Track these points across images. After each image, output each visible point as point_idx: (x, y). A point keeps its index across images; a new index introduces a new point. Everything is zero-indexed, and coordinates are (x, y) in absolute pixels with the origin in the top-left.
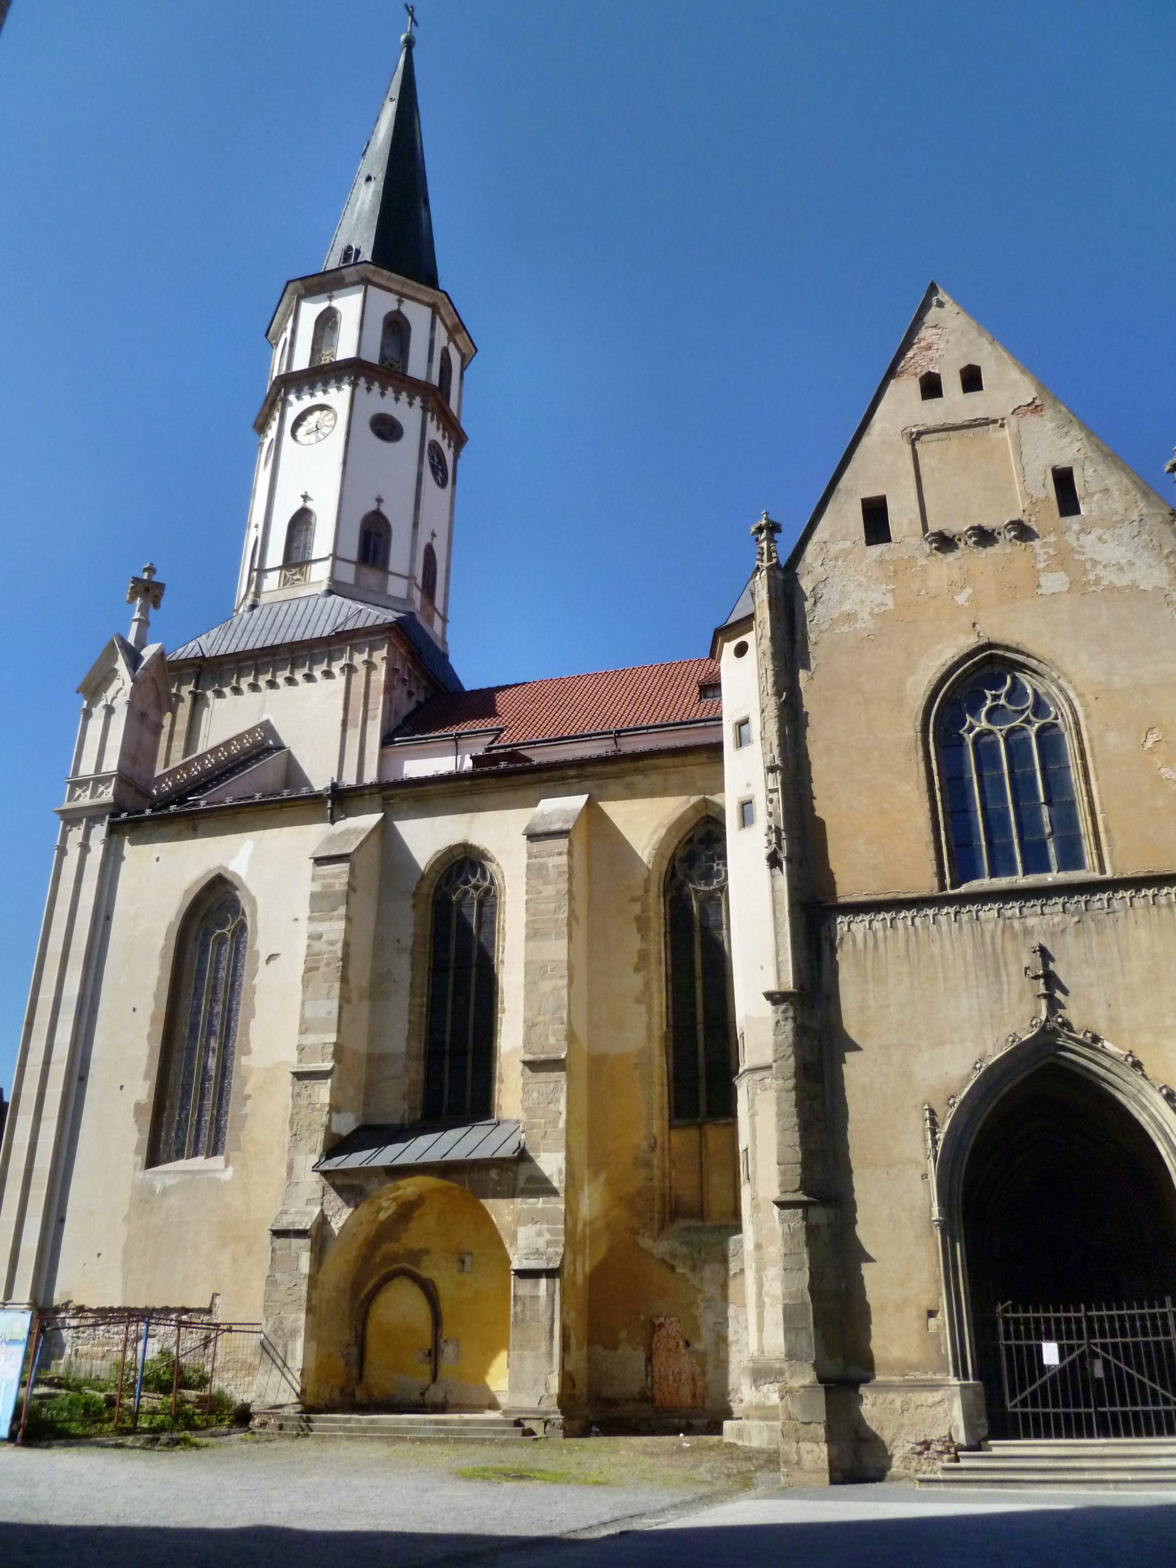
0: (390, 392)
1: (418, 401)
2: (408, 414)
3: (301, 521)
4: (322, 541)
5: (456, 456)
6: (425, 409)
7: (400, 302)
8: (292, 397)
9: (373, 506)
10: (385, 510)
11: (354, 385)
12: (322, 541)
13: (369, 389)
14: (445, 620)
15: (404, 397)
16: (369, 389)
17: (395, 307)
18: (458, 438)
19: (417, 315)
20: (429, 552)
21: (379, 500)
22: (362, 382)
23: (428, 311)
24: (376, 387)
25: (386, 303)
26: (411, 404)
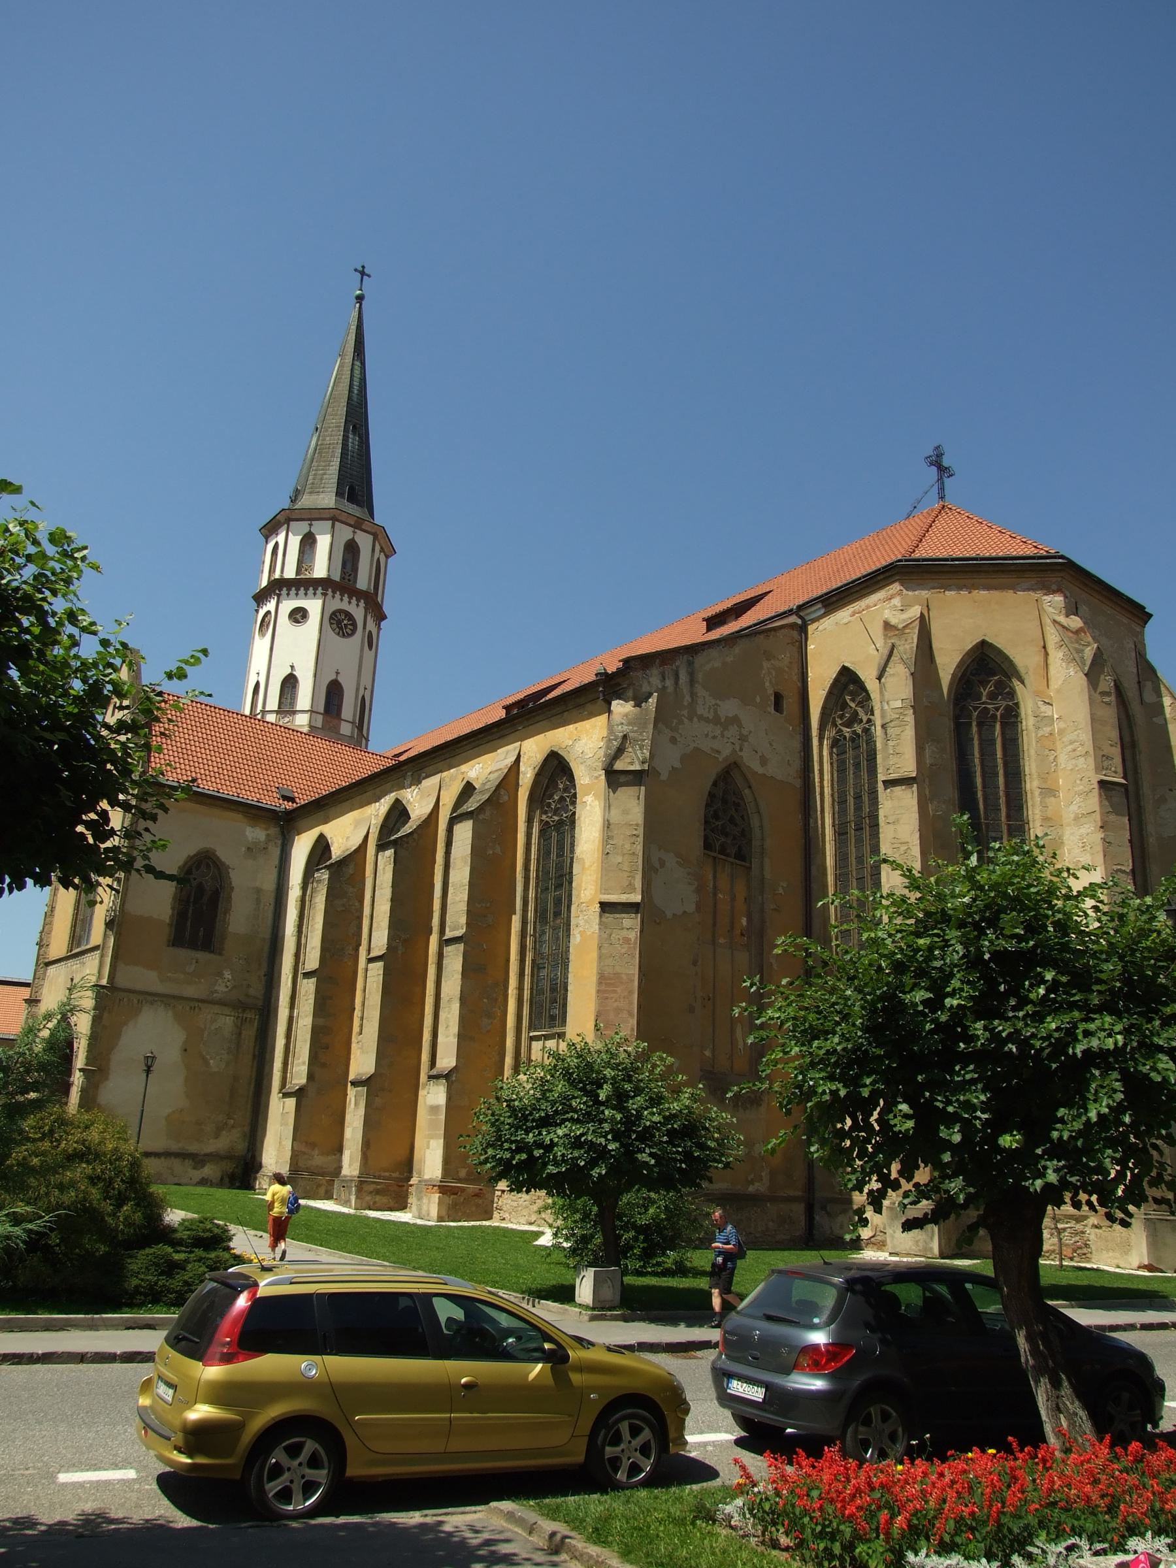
0: (346, 598)
1: (362, 604)
2: (358, 611)
3: (290, 683)
4: (304, 699)
5: (379, 629)
6: (366, 609)
7: (354, 532)
8: (284, 591)
9: (334, 677)
10: (339, 679)
11: (325, 595)
12: (304, 699)
13: (333, 597)
14: (367, 740)
15: (354, 601)
16: (333, 597)
17: (351, 537)
18: (380, 617)
19: (364, 541)
20: (363, 697)
21: (337, 673)
22: (330, 592)
23: (371, 537)
24: (338, 595)
25: (346, 533)
26: (358, 605)
